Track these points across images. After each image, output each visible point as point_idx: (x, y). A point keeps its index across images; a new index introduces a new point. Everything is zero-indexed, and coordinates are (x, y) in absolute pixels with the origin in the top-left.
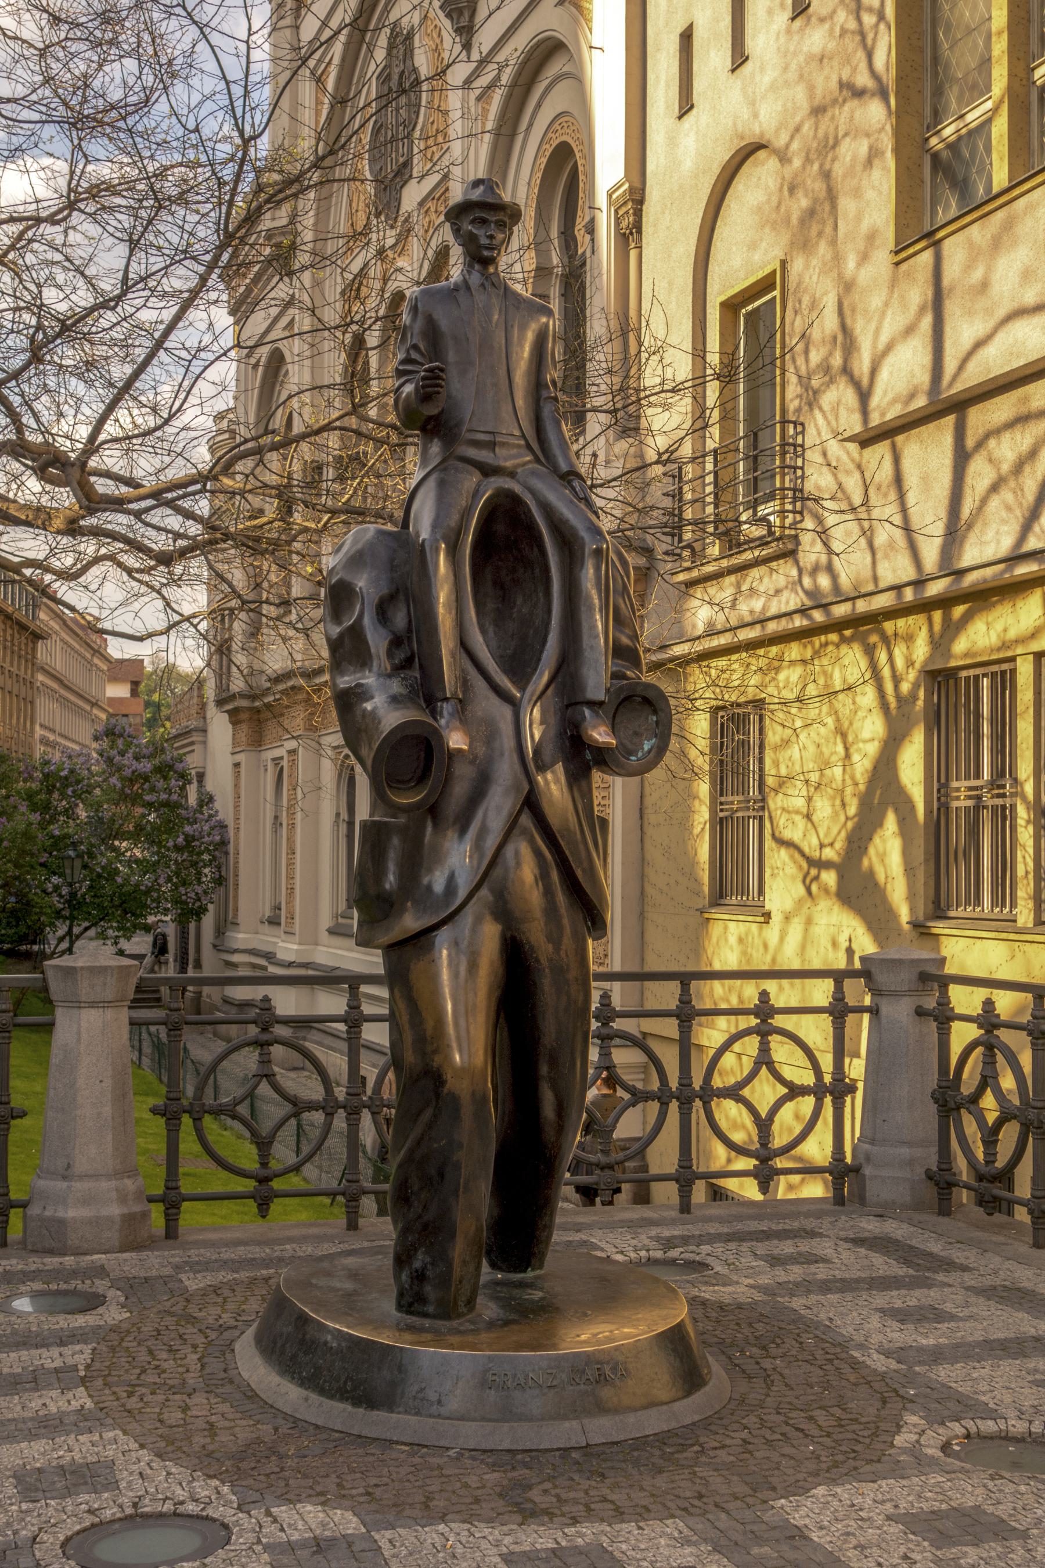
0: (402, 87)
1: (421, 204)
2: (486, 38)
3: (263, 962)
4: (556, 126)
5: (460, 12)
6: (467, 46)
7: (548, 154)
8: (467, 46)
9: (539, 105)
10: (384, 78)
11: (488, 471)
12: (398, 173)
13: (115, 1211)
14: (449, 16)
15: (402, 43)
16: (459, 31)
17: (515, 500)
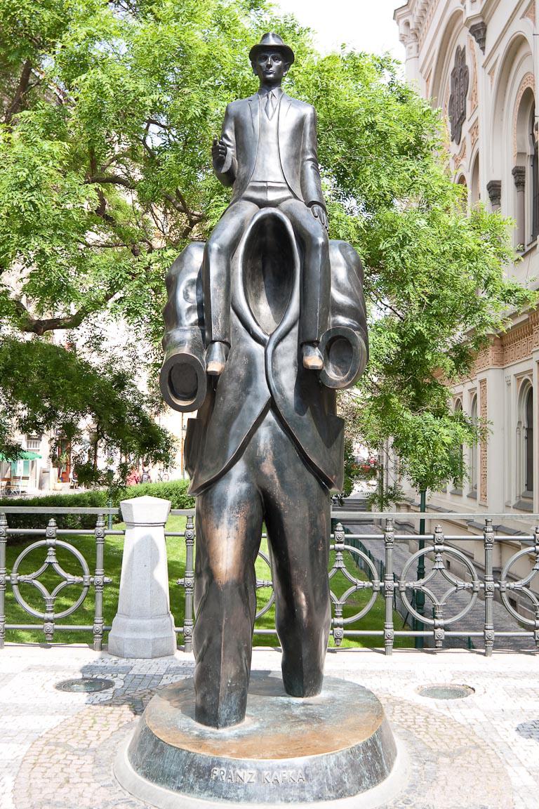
0: (461, 76)
1: (470, 131)
2: (490, 44)
3: (408, 504)
4: (525, 81)
5: (479, 31)
6: (483, 48)
7: (521, 95)
8: (483, 48)
9: (517, 70)
10: (453, 74)
11: (262, 204)
12: (461, 118)
13: (150, 636)
14: (474, 35)
15: (461, 55)
16: (478, 41)
17: (276, 220)
